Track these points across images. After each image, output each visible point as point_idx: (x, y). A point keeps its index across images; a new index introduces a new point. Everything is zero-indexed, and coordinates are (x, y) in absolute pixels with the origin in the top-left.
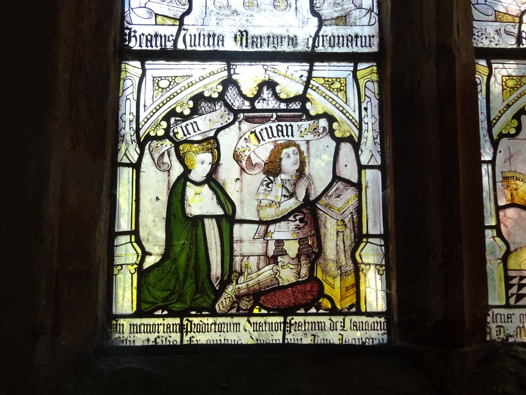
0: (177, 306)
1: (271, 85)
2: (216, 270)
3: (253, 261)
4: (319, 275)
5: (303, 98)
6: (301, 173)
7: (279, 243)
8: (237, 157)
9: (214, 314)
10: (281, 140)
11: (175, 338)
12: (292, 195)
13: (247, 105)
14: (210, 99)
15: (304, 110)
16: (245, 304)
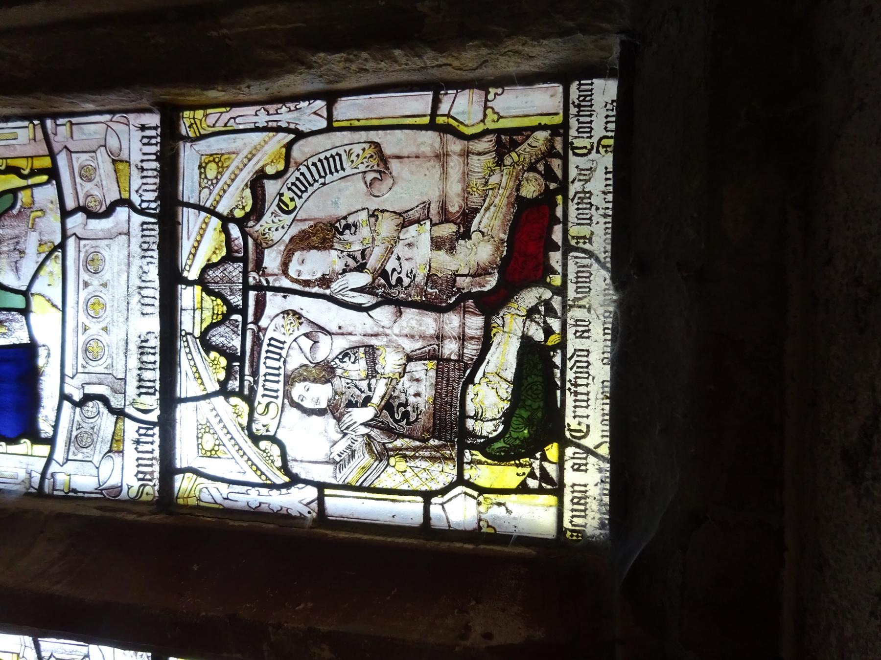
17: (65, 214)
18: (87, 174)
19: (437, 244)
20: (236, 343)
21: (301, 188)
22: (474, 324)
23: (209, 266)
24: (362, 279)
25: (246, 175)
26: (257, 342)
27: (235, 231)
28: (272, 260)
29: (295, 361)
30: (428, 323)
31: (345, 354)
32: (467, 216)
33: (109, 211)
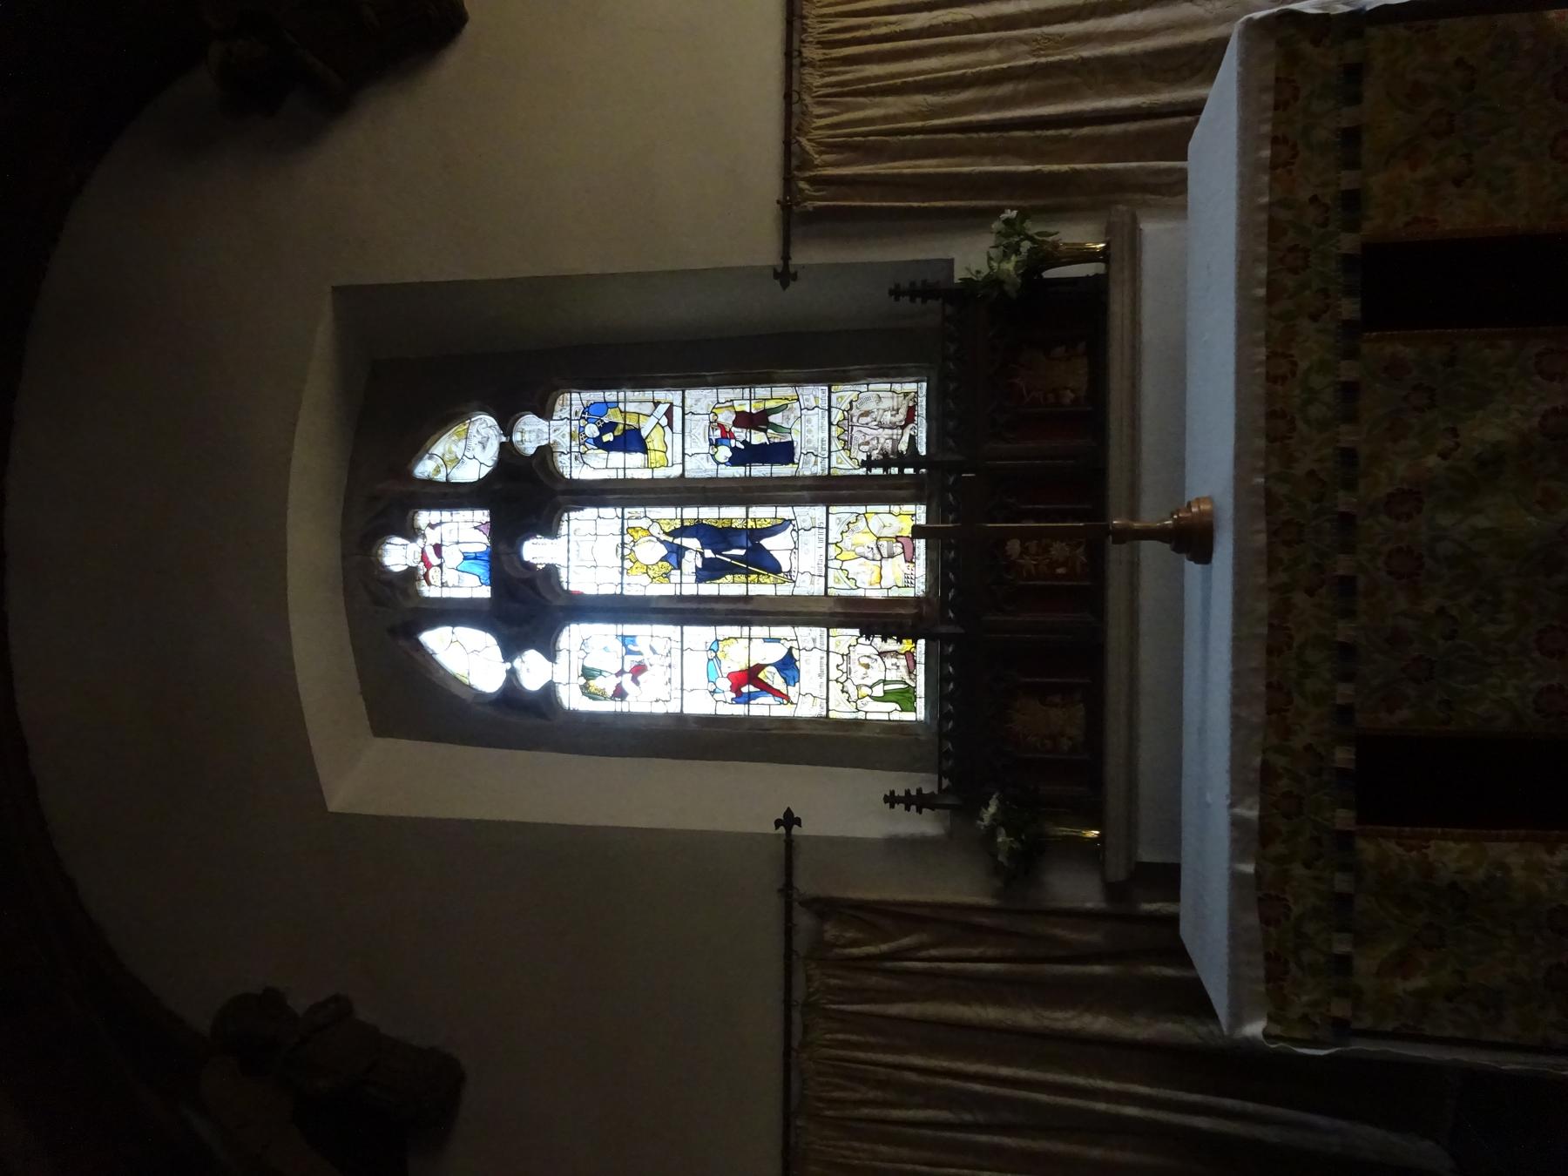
0: (913, 699)
1: (838, 666)
2: (902, 686)
3: (899, 674)
4: (903, 652)
5: (843, 655)
6: (869, 657)
7: (892, 665)
8: (863, 678)
9: (915, 687)
10: (857, 663)
11: (923, 700)
12: (876, 660)
13: (845, 675)
14: (843, 687)
15: (847, 655)
16: (913, 677)
17: (801, 410)
18: (807, 400)
19: (892, 415)
20: (846, 438)
21: (861, 404)
22: (900, 431)
23: (839, 421)
24: (876, 423)
25: (849, 400)
26: (851, 437)
27: (845, 413)
28: (855, 419)
29: (861, 441)
30: (890, 432)
31: (872, 439)
32: (898, 410)
33: (813, 409)
